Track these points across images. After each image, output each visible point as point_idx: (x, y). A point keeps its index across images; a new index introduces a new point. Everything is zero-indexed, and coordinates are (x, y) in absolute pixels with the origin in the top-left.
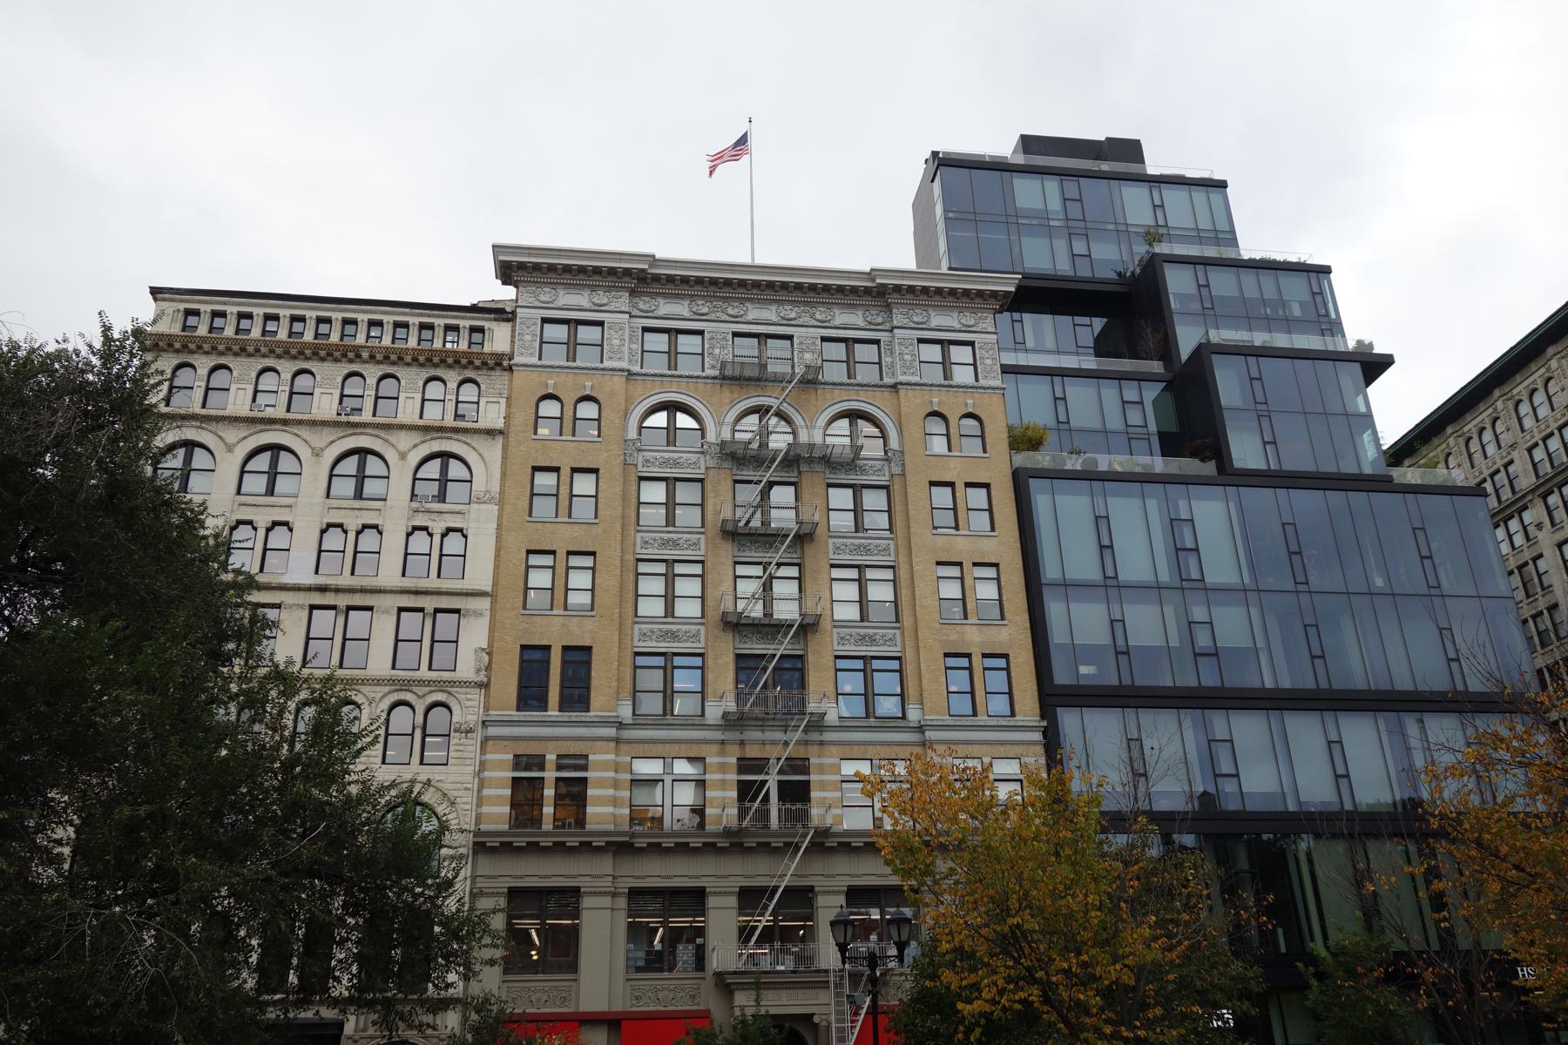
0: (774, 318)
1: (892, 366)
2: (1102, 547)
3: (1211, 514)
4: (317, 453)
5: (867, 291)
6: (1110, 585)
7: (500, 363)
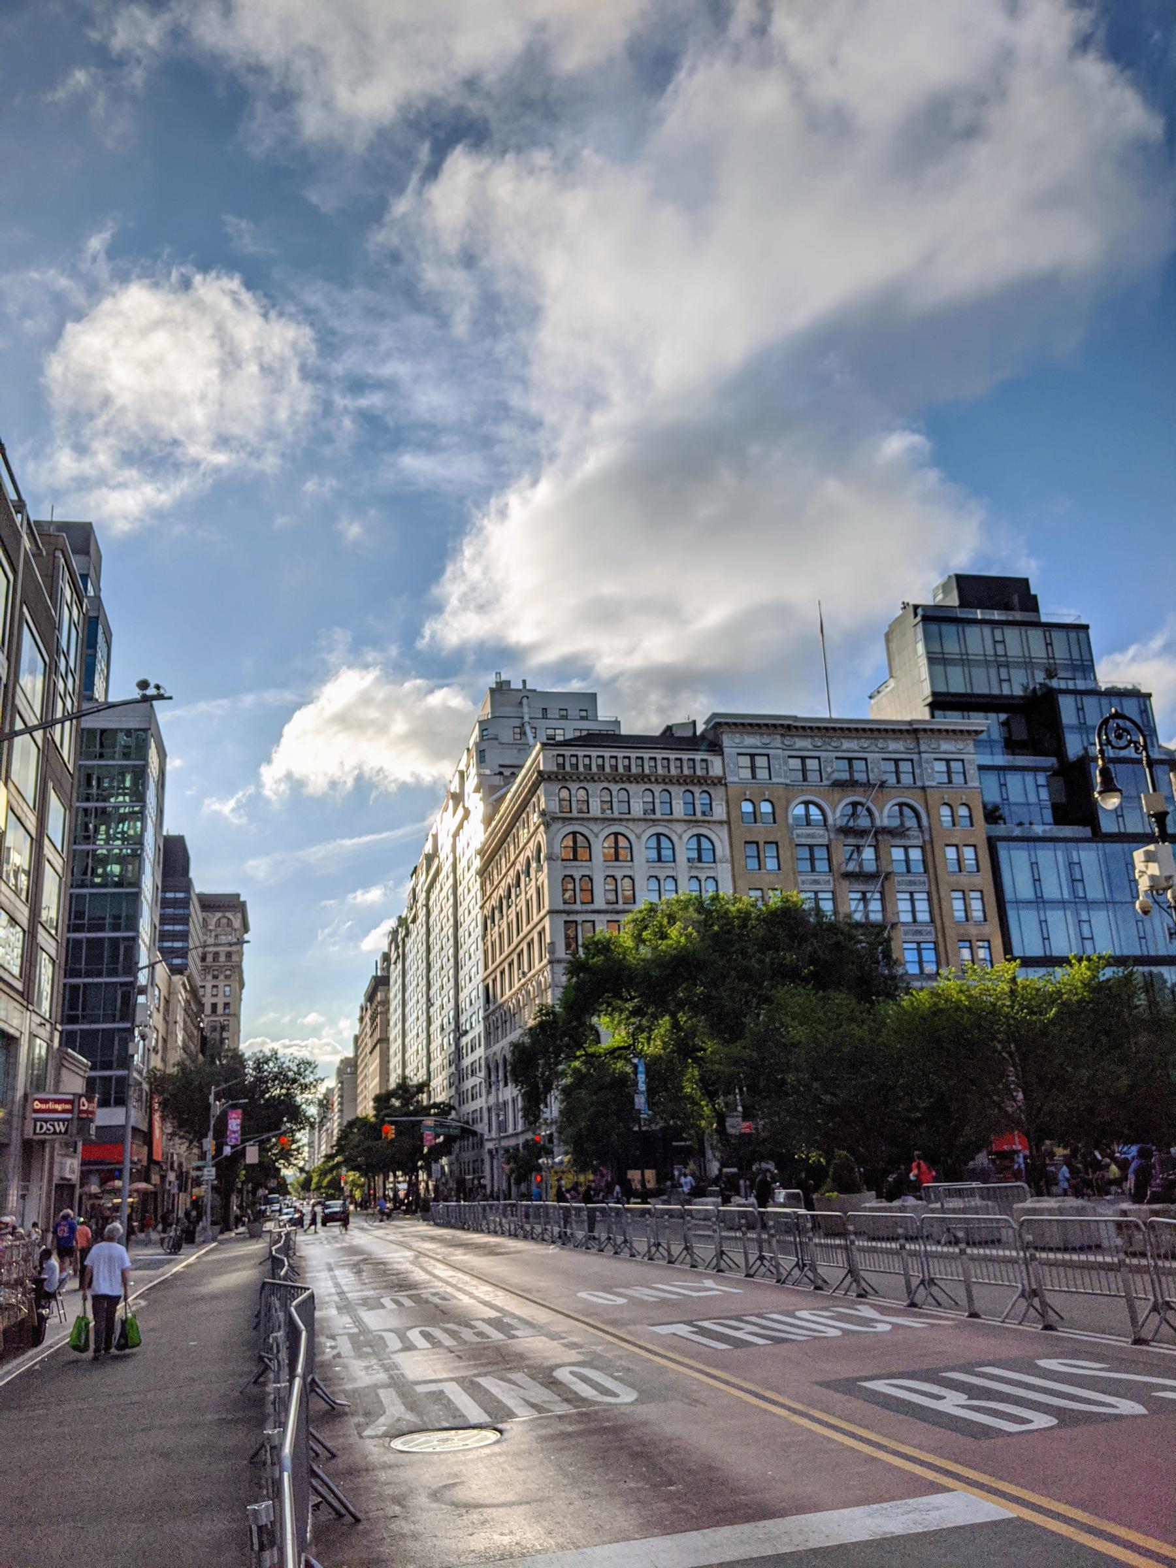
0: (856, 748)
1: (922, 774)
2: (1035, 880)
3: (1089, 857)
4: (638, 837)
5: (907, 731)
6: (1040, 902)
7: (720, 781)
